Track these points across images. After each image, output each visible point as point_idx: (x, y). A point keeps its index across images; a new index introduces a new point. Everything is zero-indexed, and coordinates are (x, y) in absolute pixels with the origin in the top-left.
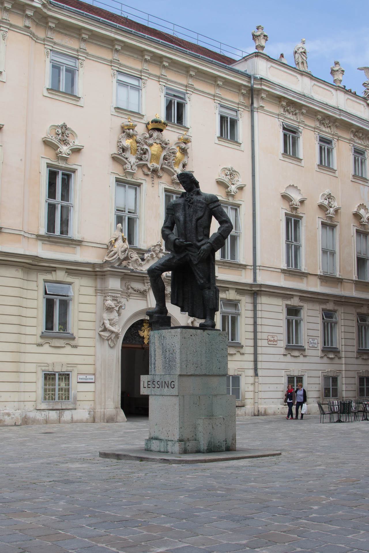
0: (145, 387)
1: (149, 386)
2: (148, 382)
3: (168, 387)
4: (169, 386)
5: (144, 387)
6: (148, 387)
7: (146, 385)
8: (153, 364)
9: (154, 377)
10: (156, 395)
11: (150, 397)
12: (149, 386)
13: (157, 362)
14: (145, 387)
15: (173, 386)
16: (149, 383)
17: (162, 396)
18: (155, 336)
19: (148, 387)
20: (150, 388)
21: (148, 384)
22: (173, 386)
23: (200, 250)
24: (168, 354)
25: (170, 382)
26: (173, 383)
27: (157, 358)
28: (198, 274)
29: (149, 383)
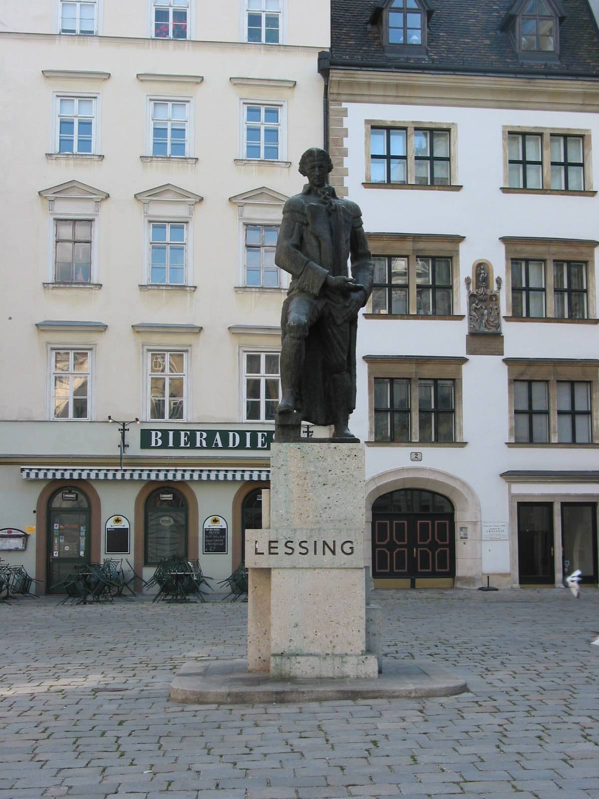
0: (263, 554)
1: (272, 551)
2: (270, 542)
3: (333, 552)
5: (257, 553)
6: (270, 553)
11: (273, 573)
12: (272, 551)
14: (263, 554)
15: (350, 551)
16: (273, 545)
17: (312, 570)
19: (270, 553)
20: (277, 553)
21: (270, 548)
22: (350, 551)
23: (350, 301)
26: (349, 545)
28: (339, 344)
29: (273, 545)
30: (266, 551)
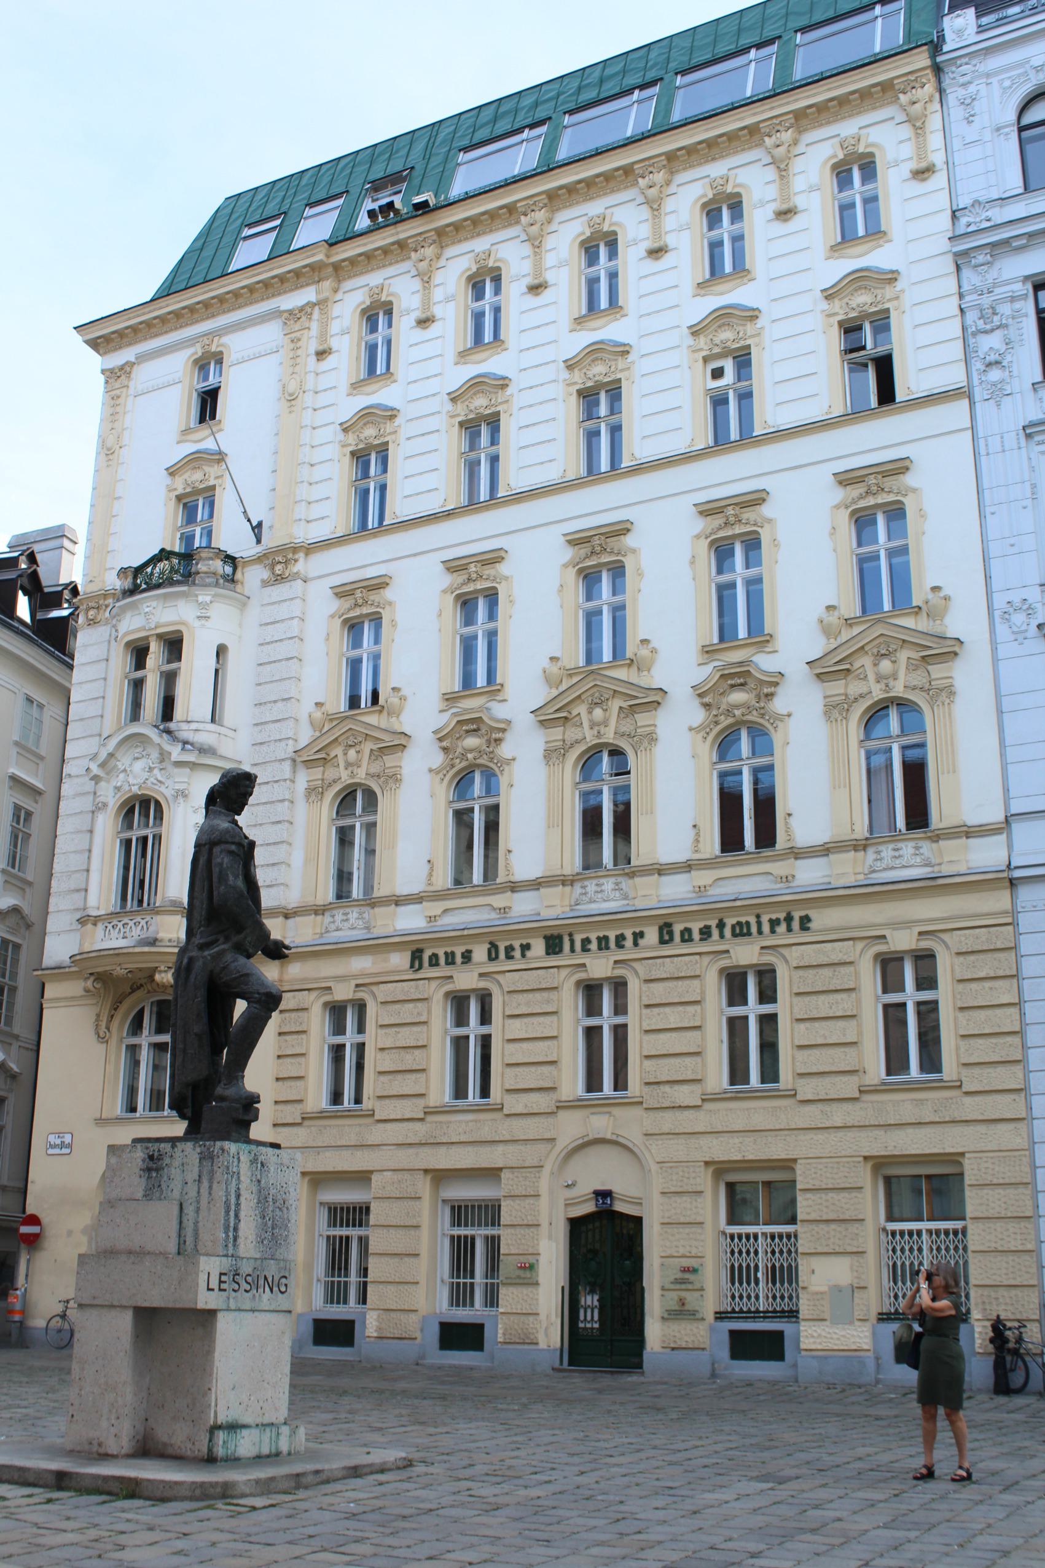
0: (213, 1290)
1: (223, 1286)
2: (221, 1274)
3: (271, 1290)
4: (275, 1289)
5: (209, 1289)
6: (220, 1290)
7: (214, 1284)
8: (231, 1229)
9: (239, 1263)
10: (240, 1310)
12: (223, 1286)
13: (242, 1226)
14: (213, 1290)
15: (283, 1289)
16: (224, 1278)
18: (242, 1158)
19: (220, 1290)
20: (225, 1290)
21: (221, 1282)
24: (271, 1209)
25: (276, 1278)
26: (284, 1281)
27: (242, 1214)
29: (224, 1278)
30: (216, 1288)
